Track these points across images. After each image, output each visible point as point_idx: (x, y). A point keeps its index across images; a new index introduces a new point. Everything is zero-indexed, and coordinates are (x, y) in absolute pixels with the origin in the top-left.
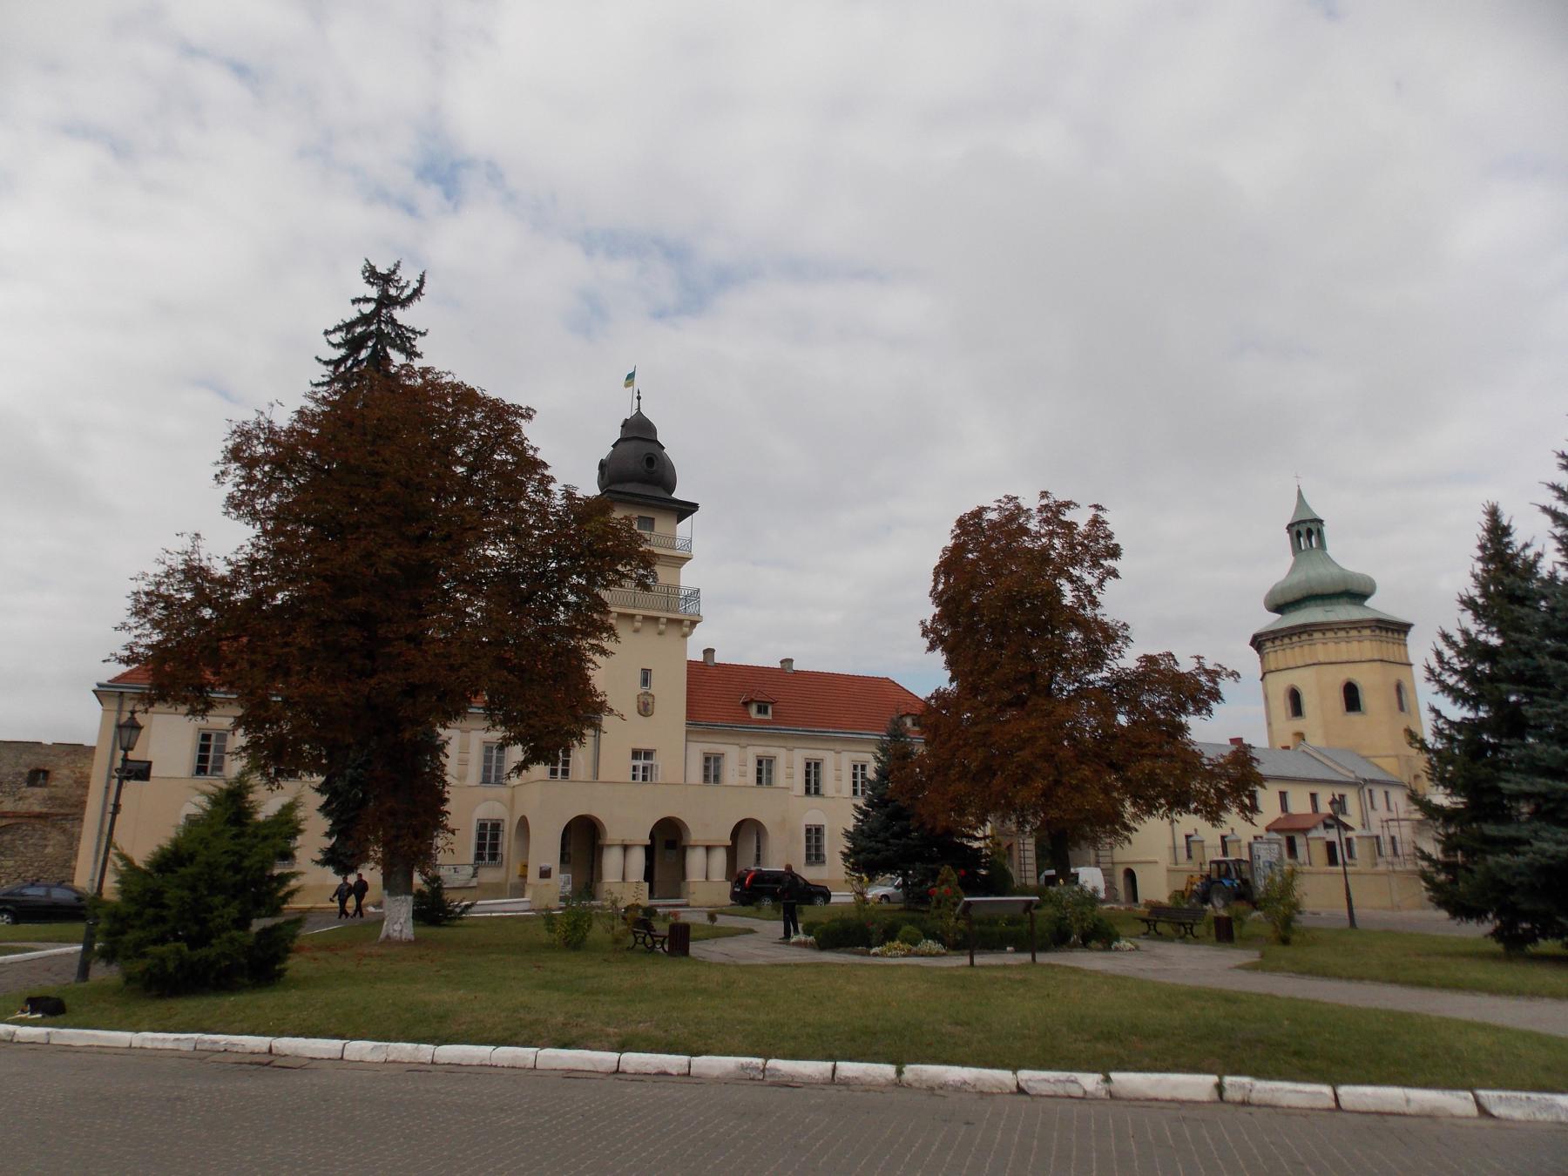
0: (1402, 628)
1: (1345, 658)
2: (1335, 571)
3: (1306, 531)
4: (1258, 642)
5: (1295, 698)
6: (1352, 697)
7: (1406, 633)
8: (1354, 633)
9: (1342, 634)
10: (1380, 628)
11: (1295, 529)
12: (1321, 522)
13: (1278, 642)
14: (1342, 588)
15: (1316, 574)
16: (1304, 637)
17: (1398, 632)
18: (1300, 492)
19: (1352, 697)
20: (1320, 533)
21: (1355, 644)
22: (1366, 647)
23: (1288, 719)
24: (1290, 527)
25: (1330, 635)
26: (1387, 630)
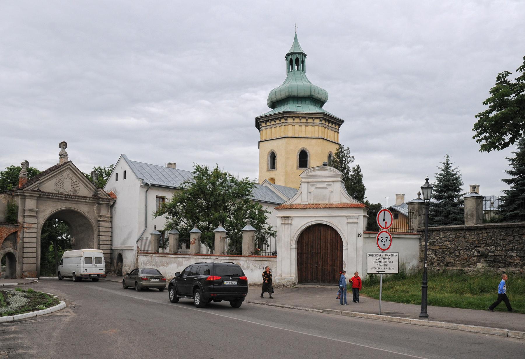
0: (338, 122)
1: (303, 136)
2: (305, 83)
3: (296, 60)
4: (259, 123)
5: (273, 157)
6: (303, 159)
7: (339, 125)
8: (310, 121)
9: (304, 120)
10: (325, 120)
11: (290, 57)
12: (305, 56)
13: (268, 124)
14: (307, 94)
15: (298, 84)
16: (283, 120)
17: (335, 123)
18: (296, 35)
19: (303, 159)
20: (303, 62)
21: (310, 127)
22: (316, 129)
23: (268, 170)
24: (288, 55)
25: (297, 120)
26: (329, 122)
